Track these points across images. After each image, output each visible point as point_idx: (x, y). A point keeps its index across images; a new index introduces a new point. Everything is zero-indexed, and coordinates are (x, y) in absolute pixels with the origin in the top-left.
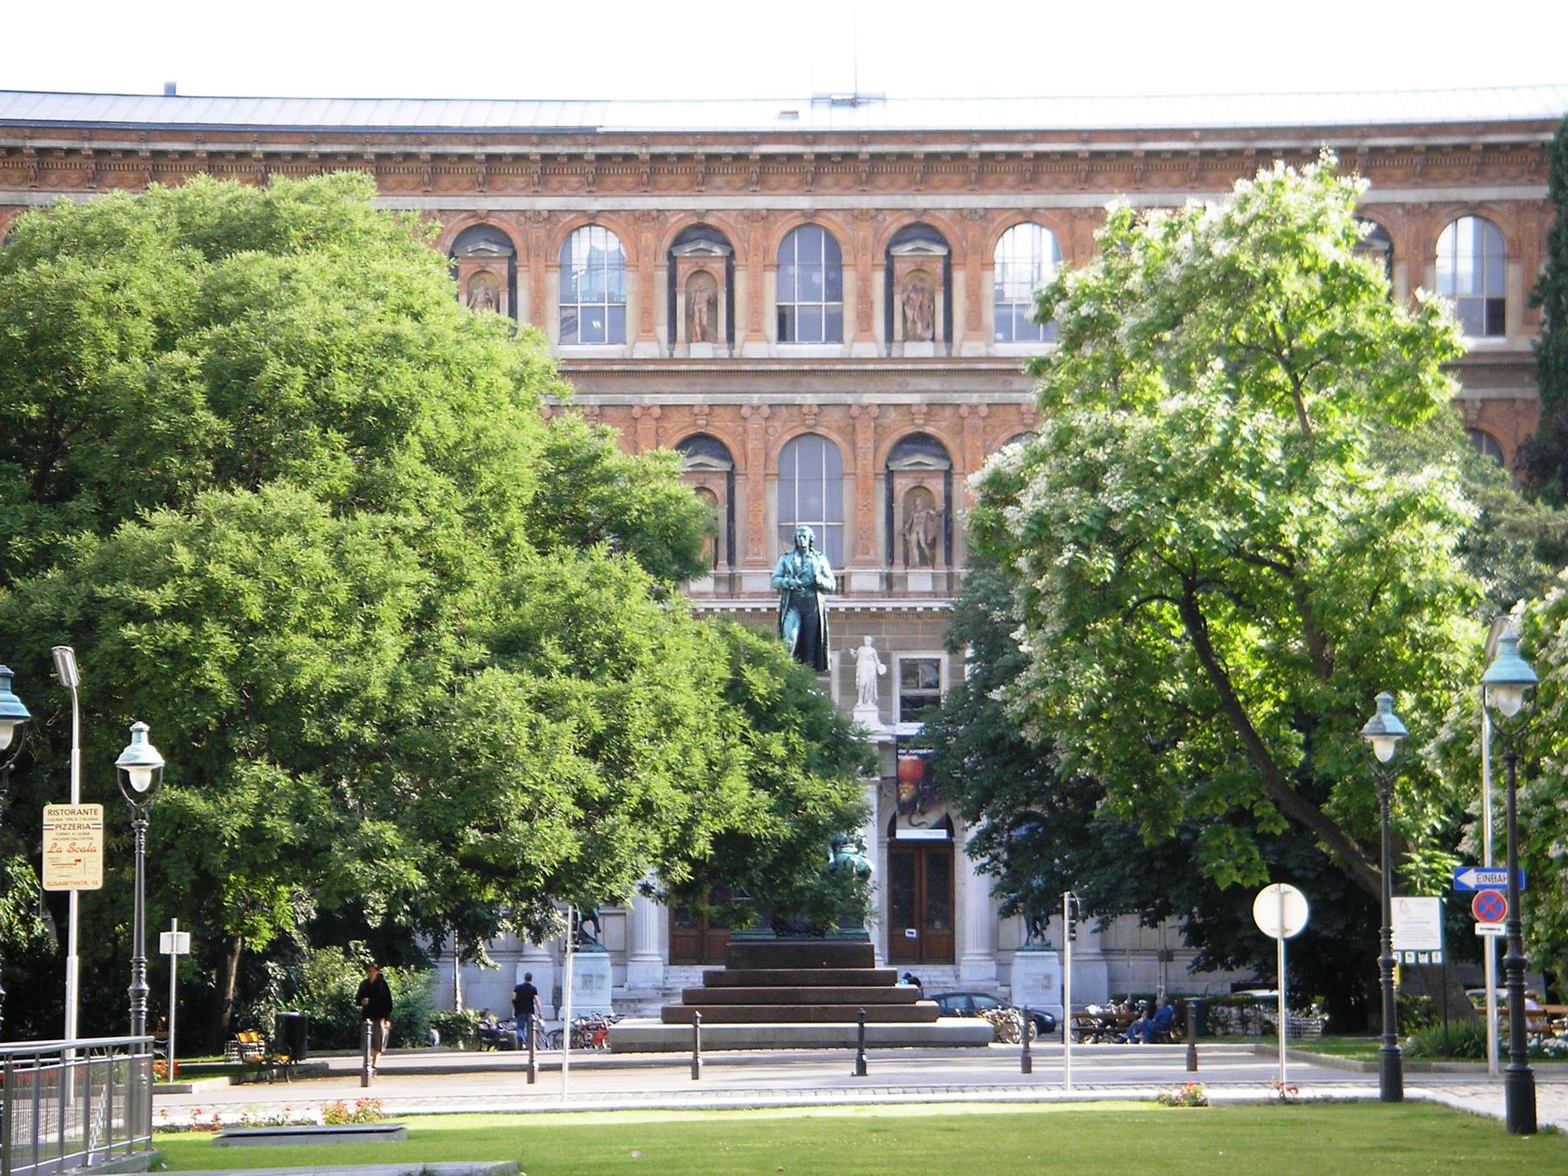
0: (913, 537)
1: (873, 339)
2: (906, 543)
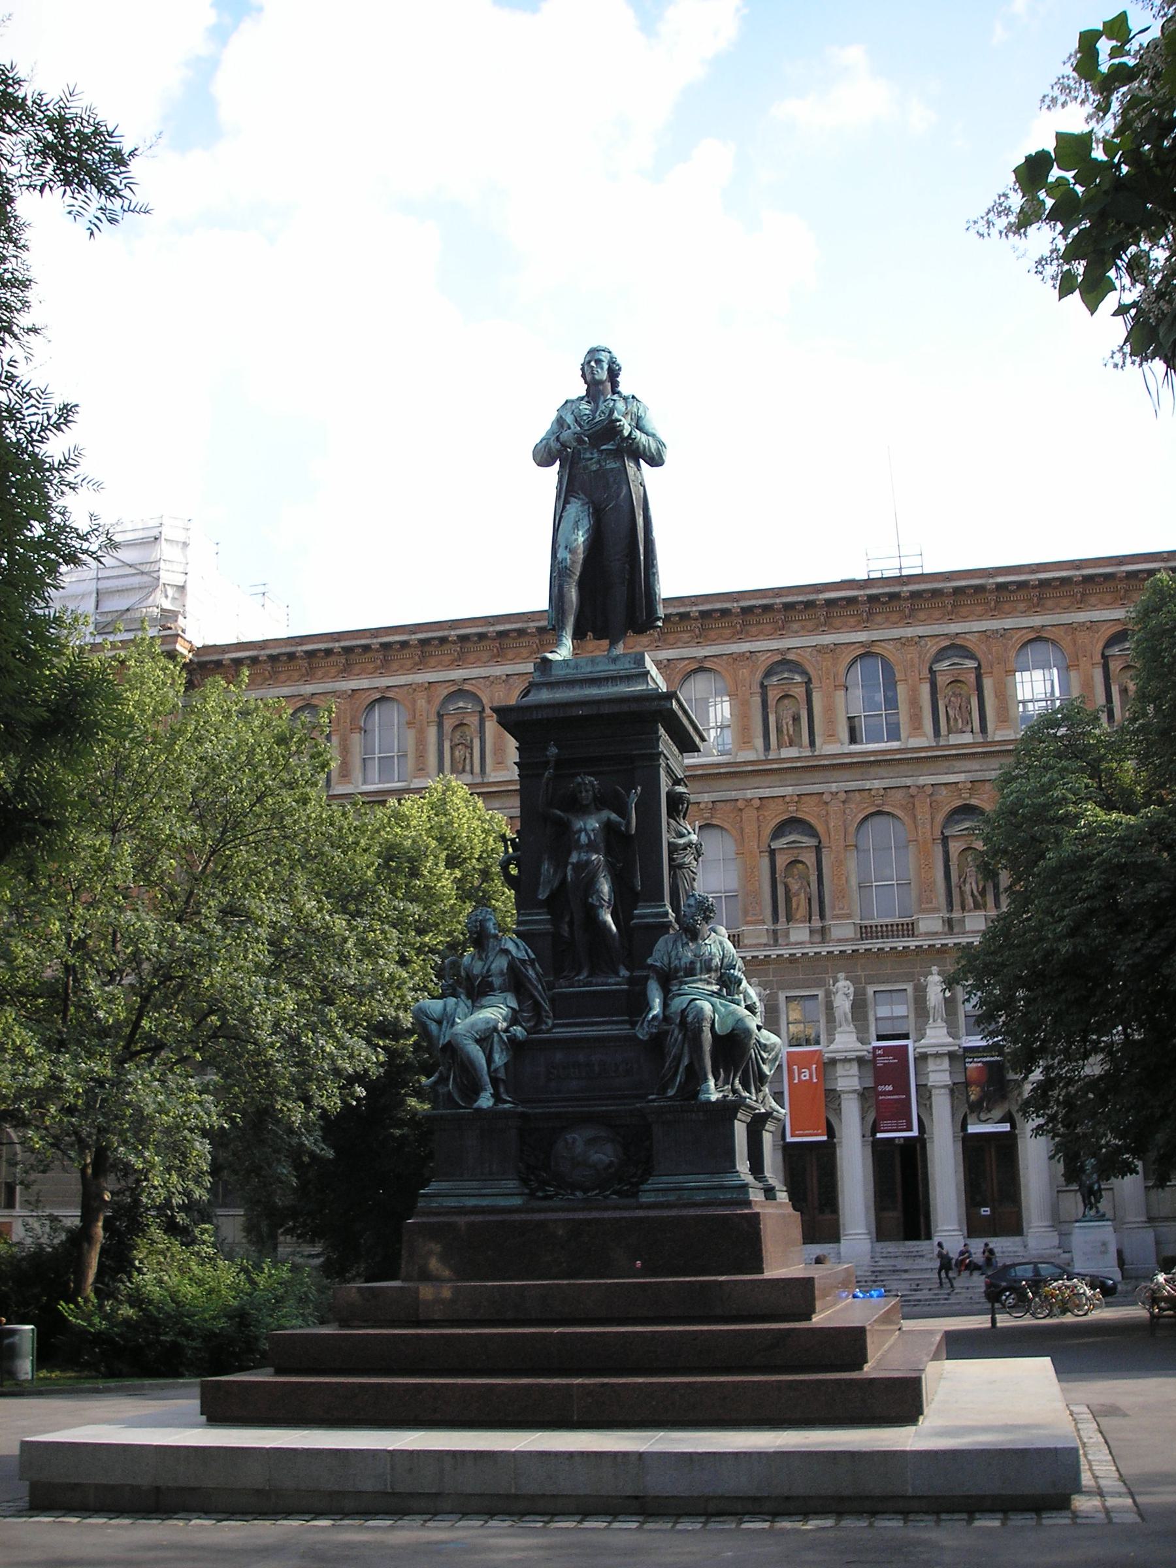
0: (967, 888)
1: (925, 735)
2: (962, 893)
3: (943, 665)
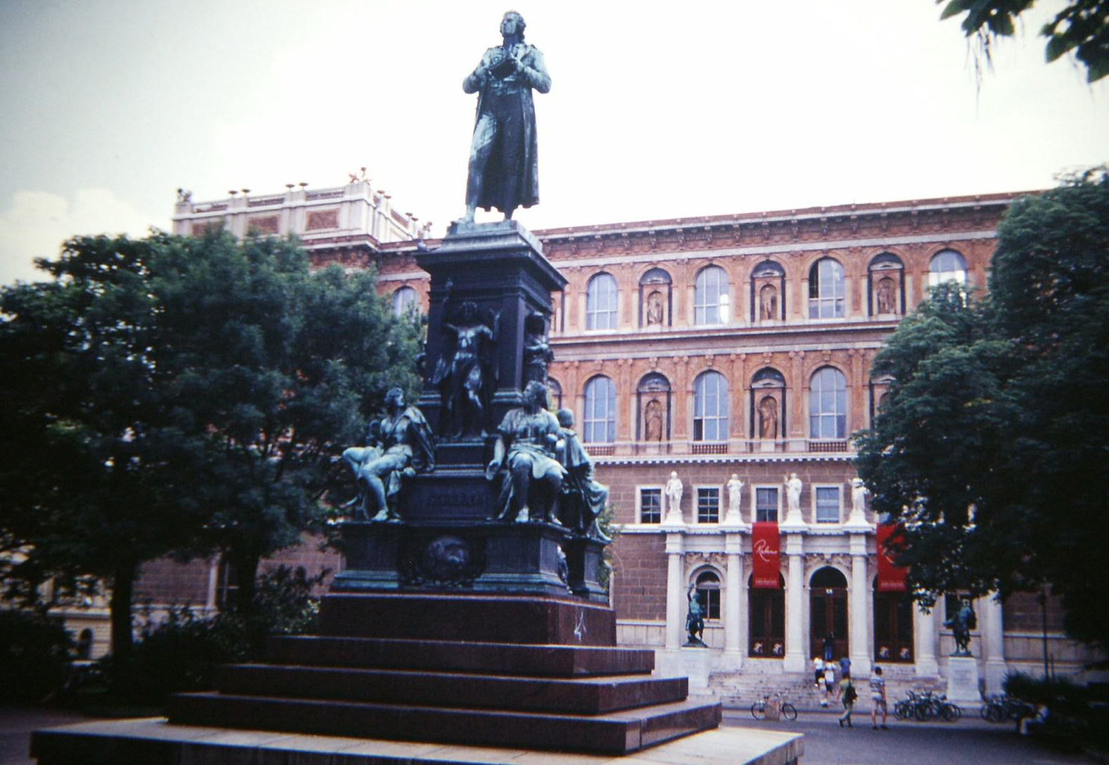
3: (878, 267)
